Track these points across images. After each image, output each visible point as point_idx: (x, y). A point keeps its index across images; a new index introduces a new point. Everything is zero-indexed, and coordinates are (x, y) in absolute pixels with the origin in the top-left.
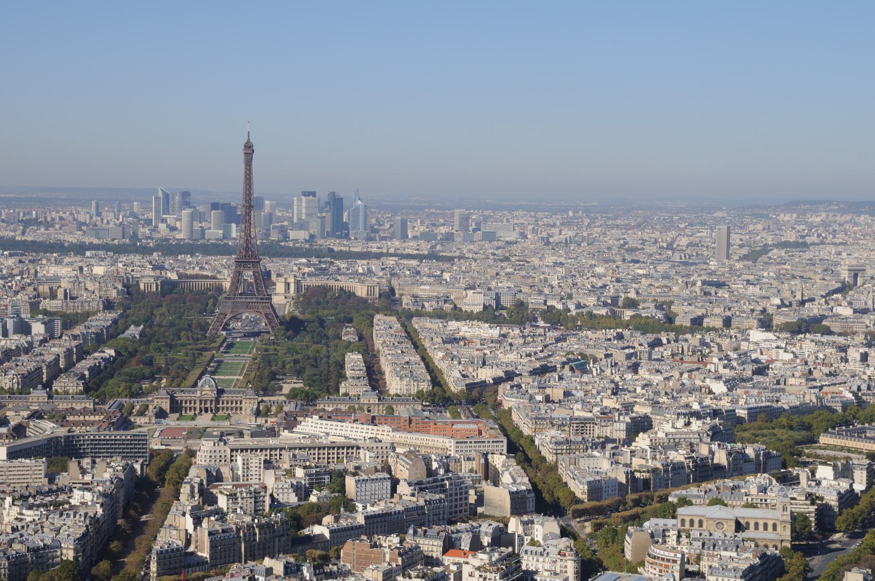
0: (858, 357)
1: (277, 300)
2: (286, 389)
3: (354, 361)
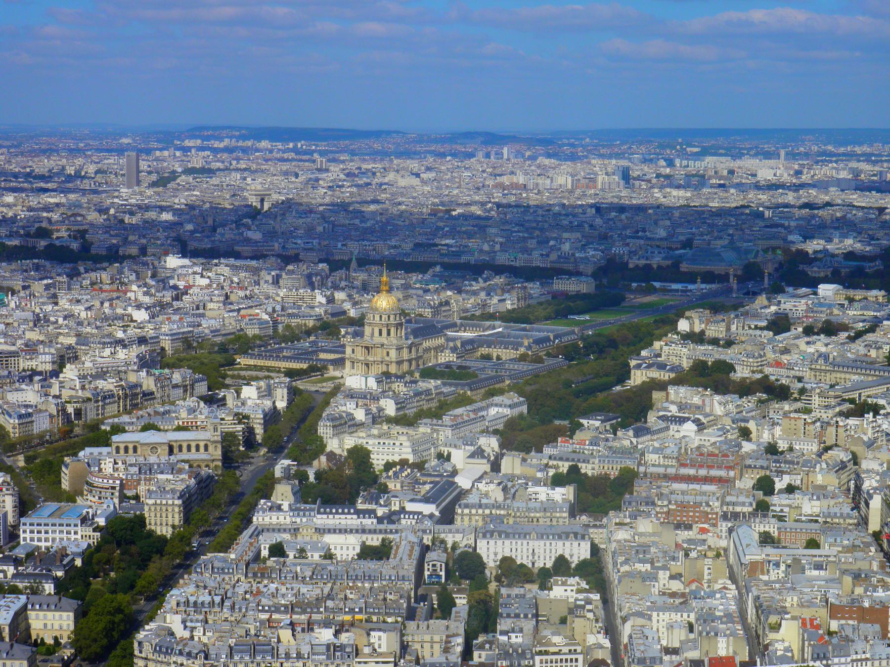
0: (269, 278)
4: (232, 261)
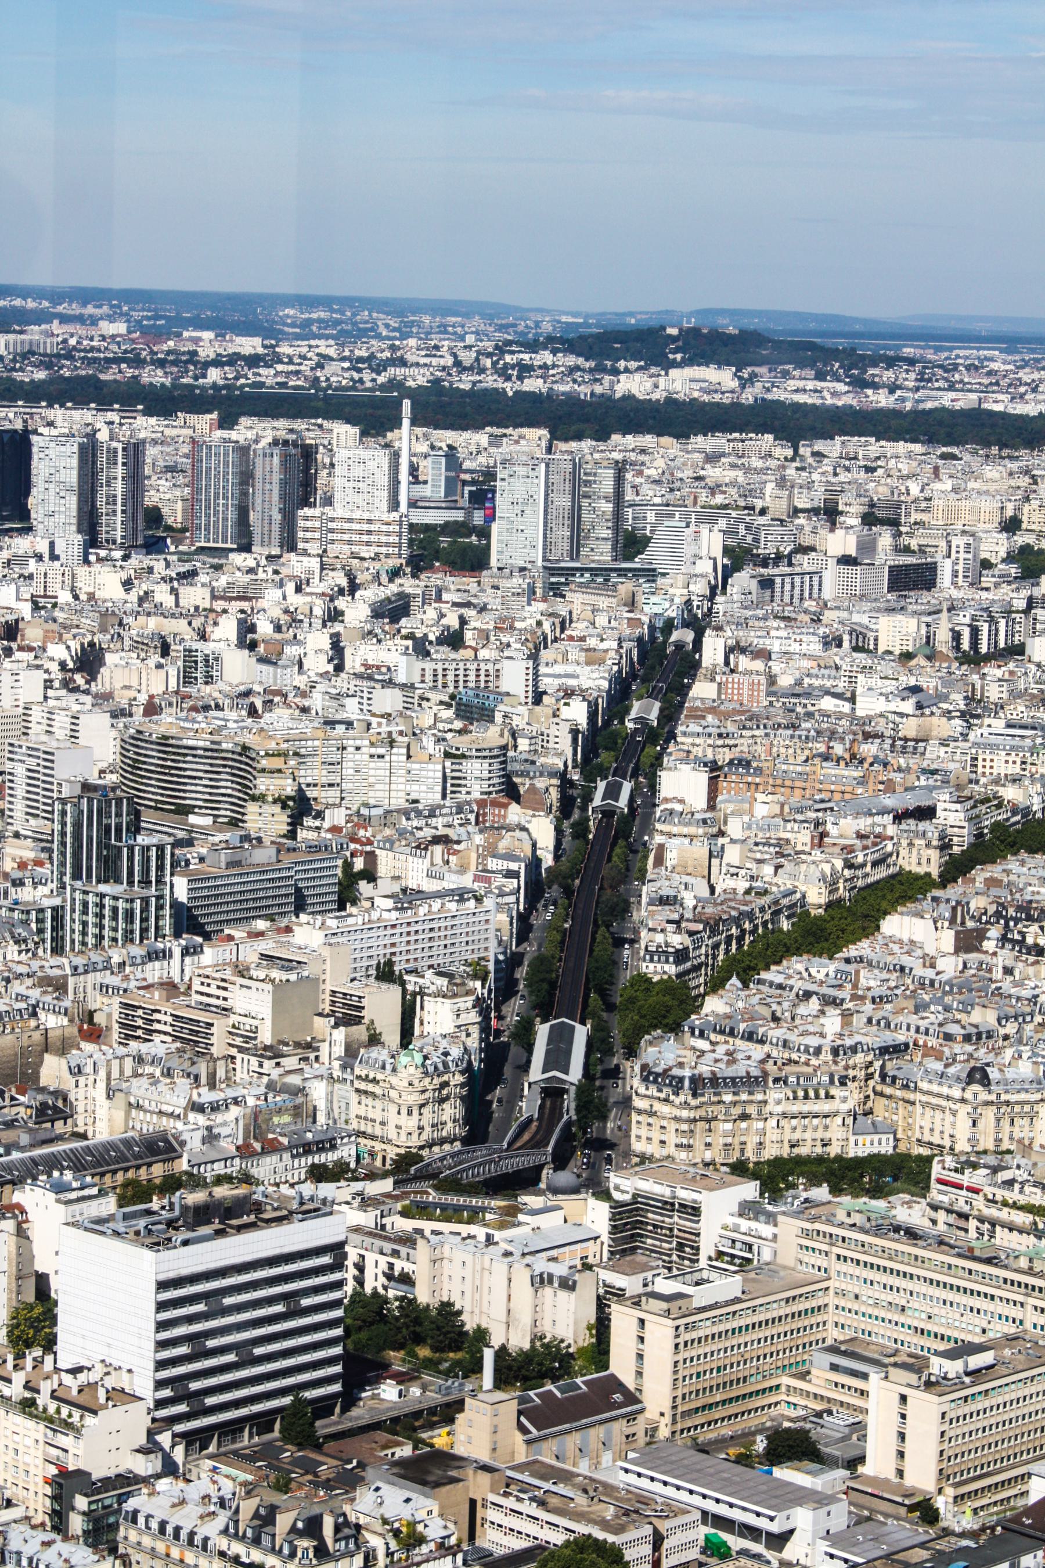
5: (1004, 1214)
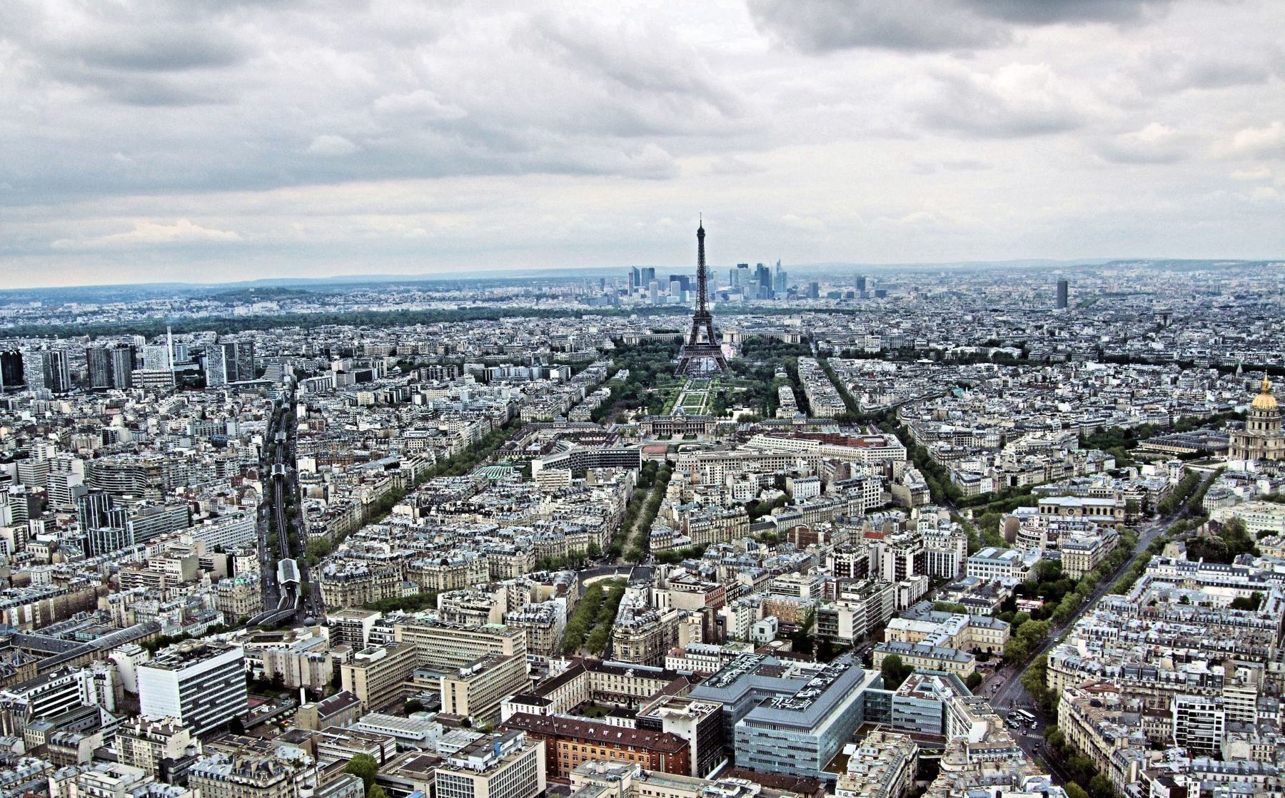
0: (1169, 380)
1: (723, 347)
2: (737, 414)
3: (786, 393)
4: (1138, 366)
5: (468, 611)
